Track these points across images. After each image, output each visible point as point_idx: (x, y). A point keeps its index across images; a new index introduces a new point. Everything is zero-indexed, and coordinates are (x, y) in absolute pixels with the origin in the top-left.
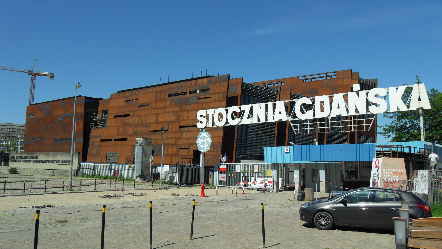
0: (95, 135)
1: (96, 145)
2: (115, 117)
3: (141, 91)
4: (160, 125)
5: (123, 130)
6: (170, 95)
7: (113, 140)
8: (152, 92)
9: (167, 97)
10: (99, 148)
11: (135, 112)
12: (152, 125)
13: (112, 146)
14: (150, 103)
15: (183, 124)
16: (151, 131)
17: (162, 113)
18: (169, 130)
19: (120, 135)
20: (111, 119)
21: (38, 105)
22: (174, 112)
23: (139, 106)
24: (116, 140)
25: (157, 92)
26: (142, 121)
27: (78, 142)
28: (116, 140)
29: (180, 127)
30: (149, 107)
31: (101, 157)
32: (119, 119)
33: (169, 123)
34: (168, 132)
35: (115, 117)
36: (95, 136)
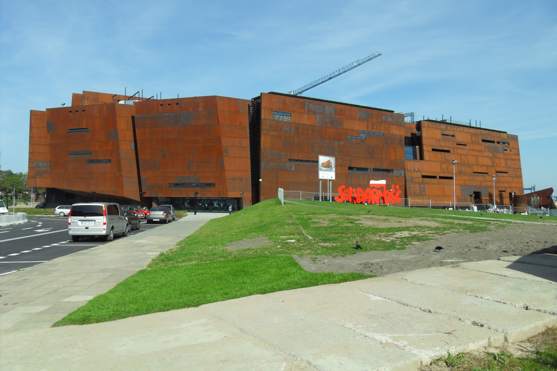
0: (411, 169)
1: (417, 181)
2: (433, 150)
3: (459, 129)
4: (481, 167)
5: (447, 167)
6: (483, 141)
7: (438, 177)
8: (467, 133)
9: (481, 142)
10: (422, 186)
11: (455, 150)
12: (474, 167)
13: (438, 184)
14: (468, 143)
15: (498, 170)
16: (474, 172)
17: (480, 156)
18: (489, 174)
19: (444, 172)
20: (429, 151)
21: (304, 100)
22: (490, 157)
23: (457, 144)
24: (441, 178)
25: (472, 134)
26: (464, 161)
27: (397, 177)
28: (441, 178)
29: (496, 172)
30: (468, 147)
31: (428, 197)
32: (439, 154)
33: (488, 166)
34: (489, 175)
35: (433, 150)
36: (413, 169)
